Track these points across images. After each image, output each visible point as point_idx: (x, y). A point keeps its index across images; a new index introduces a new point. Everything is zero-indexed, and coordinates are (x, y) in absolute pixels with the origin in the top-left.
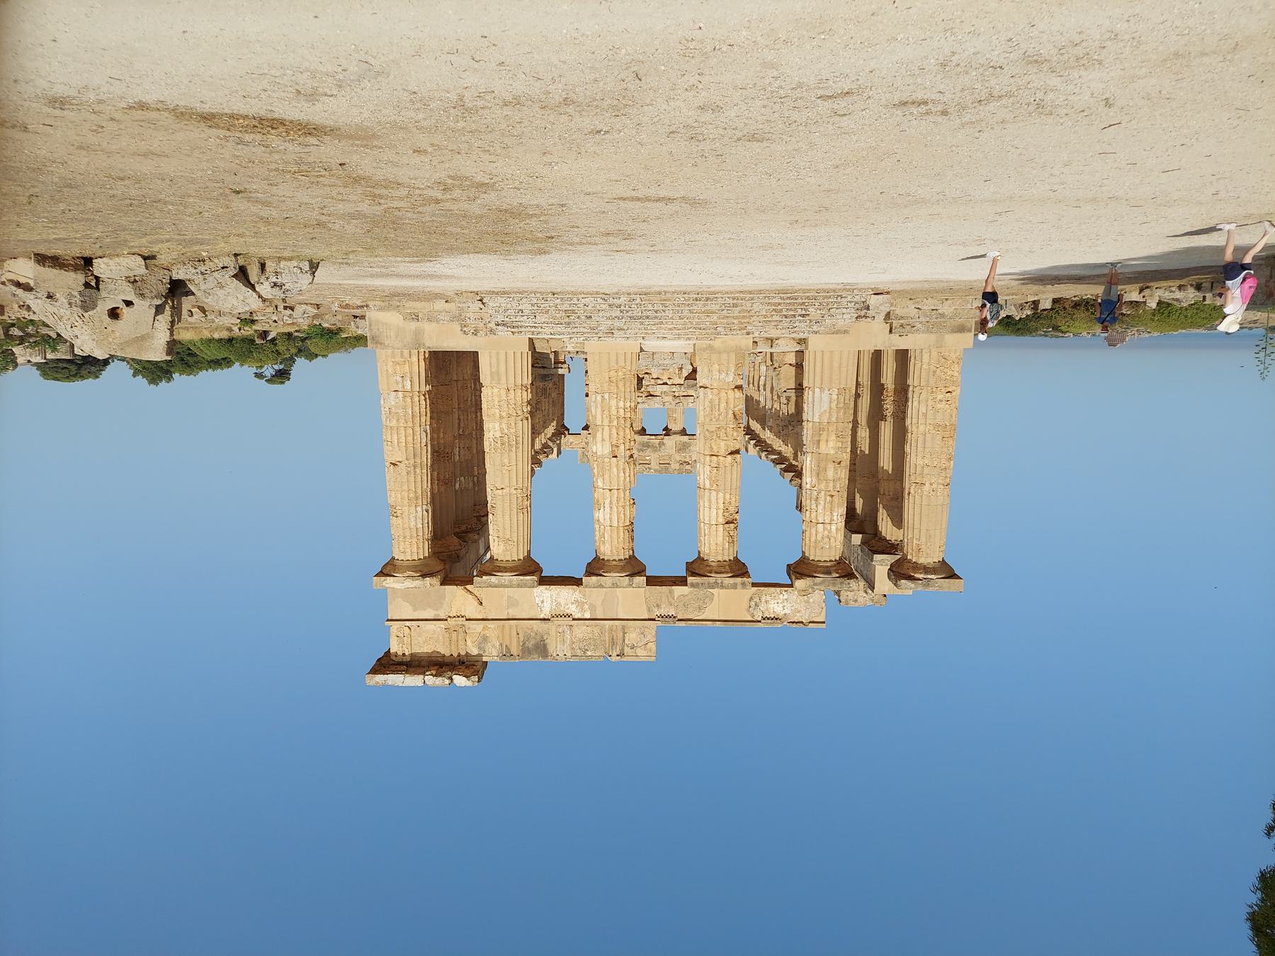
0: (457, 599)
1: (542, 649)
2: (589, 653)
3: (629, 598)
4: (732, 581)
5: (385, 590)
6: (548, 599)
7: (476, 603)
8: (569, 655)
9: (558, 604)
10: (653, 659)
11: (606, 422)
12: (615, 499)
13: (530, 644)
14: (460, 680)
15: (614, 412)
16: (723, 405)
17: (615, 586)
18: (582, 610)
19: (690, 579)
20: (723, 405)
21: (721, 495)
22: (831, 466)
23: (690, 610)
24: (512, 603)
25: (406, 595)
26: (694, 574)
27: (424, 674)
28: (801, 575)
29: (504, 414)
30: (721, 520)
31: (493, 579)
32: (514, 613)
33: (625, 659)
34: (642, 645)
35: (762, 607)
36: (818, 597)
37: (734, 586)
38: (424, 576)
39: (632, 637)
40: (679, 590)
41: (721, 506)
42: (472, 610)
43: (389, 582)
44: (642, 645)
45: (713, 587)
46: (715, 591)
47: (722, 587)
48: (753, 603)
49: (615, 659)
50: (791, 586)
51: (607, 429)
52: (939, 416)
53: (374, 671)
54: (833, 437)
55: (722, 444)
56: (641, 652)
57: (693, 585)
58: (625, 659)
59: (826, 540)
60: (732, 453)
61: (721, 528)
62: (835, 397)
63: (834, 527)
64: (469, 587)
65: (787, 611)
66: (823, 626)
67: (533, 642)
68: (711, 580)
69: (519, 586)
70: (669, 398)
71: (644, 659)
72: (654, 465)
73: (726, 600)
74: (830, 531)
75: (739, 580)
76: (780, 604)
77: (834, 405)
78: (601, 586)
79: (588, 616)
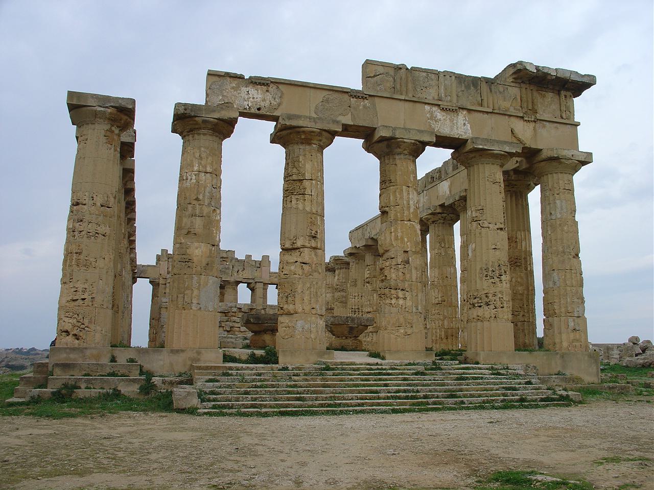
4: (300, 123)
7: (516, 131)
9: (451, 121)
12: (406, 213)
16: (306, 298)
17: (408, 130)
18: (432, 113)
20: (306, 298)
51: (414, 279)
54: (195, 259)
57: (338, 122)
59: (204, 155)
61: (308, 176)
62: (195, 301)
63: (196, 168)
65: (244, 89)
74: (200, 164)
75: (294, 123)
77: (196, 292)
79: (427, 107)
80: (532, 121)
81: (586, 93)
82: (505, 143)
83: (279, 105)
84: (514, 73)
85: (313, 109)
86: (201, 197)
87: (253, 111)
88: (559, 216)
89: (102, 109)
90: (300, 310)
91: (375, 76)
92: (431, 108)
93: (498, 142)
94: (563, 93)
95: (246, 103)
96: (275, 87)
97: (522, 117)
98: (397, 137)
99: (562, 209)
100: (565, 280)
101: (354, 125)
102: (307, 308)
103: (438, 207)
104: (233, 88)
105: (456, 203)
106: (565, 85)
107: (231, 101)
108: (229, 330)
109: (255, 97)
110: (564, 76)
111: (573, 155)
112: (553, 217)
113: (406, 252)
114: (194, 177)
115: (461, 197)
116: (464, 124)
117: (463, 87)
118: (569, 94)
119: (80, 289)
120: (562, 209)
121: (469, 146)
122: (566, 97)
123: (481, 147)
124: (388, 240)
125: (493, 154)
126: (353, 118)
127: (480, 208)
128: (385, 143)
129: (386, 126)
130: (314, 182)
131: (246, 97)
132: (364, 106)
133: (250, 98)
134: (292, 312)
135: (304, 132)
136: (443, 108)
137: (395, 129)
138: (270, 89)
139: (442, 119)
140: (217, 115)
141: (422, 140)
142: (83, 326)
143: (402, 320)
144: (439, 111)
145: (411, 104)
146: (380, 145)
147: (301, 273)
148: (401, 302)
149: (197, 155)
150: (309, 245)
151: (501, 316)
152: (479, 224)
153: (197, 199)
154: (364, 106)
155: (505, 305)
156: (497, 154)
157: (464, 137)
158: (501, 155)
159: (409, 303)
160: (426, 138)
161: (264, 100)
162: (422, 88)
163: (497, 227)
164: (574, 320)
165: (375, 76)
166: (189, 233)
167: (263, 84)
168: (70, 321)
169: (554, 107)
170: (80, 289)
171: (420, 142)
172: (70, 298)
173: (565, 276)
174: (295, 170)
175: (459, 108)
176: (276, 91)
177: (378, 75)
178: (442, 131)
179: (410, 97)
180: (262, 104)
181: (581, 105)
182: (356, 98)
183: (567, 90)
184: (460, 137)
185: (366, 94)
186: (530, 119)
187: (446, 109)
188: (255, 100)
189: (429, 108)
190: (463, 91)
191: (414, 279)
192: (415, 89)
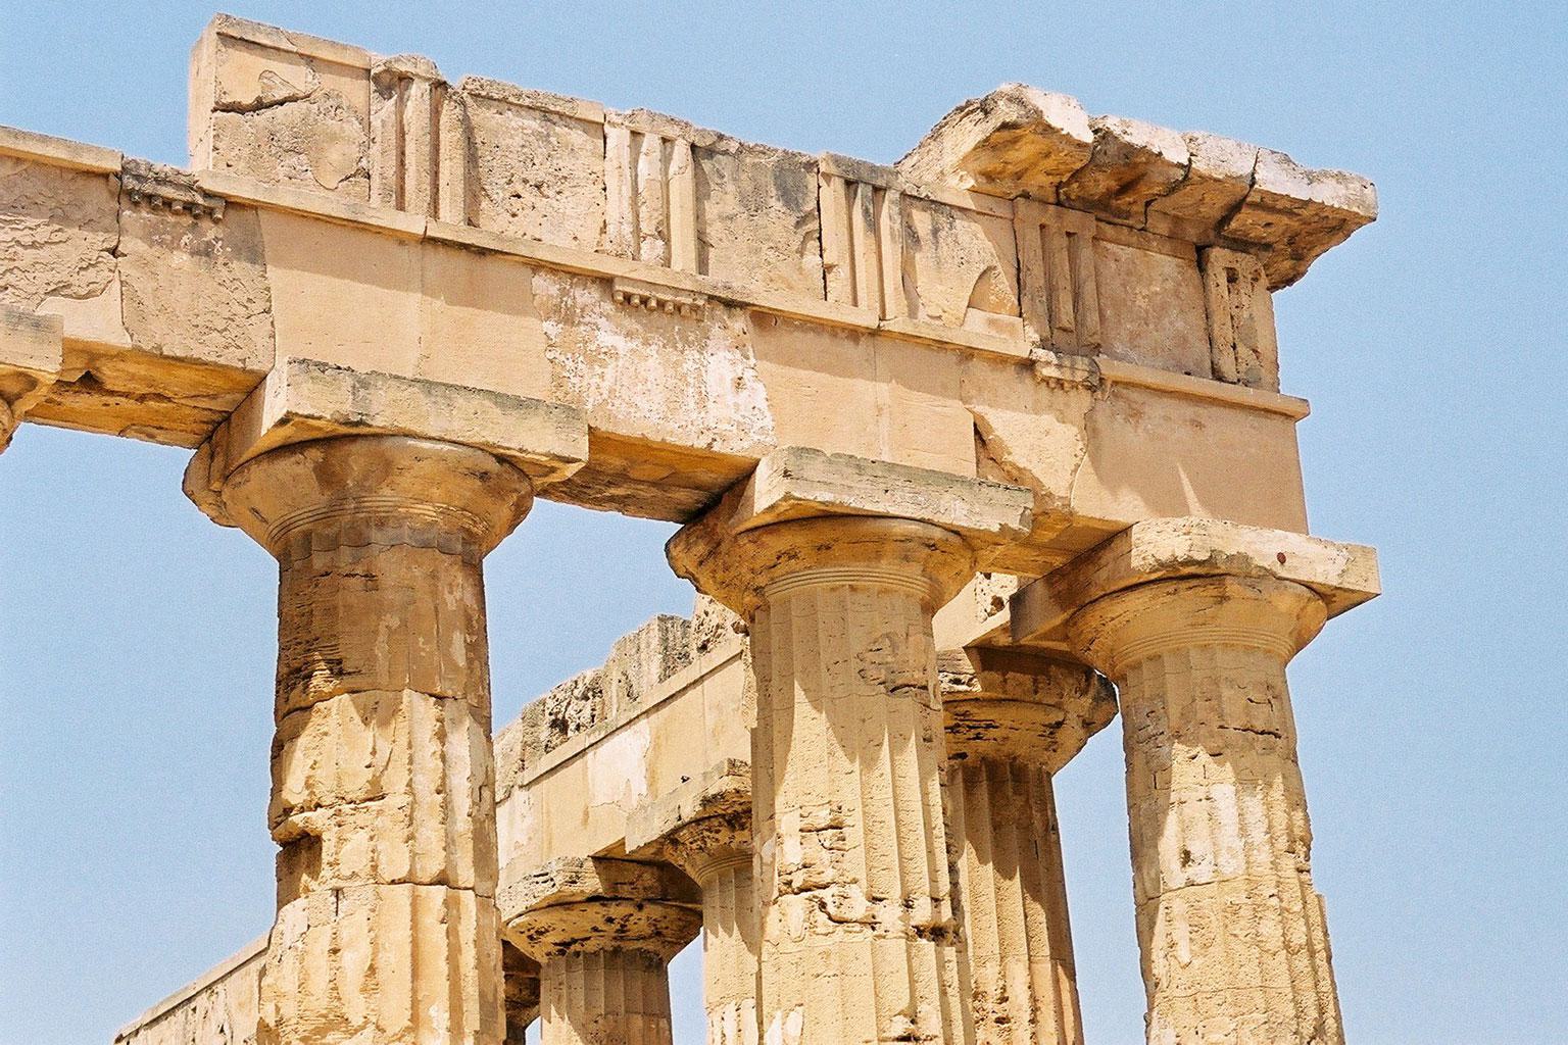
57: (41, 326)
80: (1074, 386)
81: (1325, 266)
82: (951, 480)
84: (986, 144)
91: (259, 106)
92: (564, 292)
94: (1219, 257)
97: (1028, 365)
98: (379, 422)
103: (590, 864)
105: (684, 835)
106: (1225, 220)
111: (1282, 558)
112: (1201, 871)
115: (706, 802)
117: (729, 198)
118: (1245, 263)
121: (765, 493)
122: (1232, 278)
123: (822, 496)
124: (319, 984)
127: (823, 817)
128: (315, 454)
129: (323, 367)
136: (628, 298)
144: (608, 307)
145: (461, 260)
146: (285, 466)
152: (823, 906)
157: (736, 447)
160: (536, 439)
162: (519, 188)
165: (259, 106)
169: (1180, 325)
175: (711, 298)
177: (281, 103)
178: (620, 409)
179: (450, 223)
181: (1307, 323)
182: (155, 209)
183: (1240, 244)
184: (716, 447)
185: (207, 195)
186: (1067, 375)
187: (644, 301)
189: (554, 290)
190: (731, 218)
192: (474, 191)
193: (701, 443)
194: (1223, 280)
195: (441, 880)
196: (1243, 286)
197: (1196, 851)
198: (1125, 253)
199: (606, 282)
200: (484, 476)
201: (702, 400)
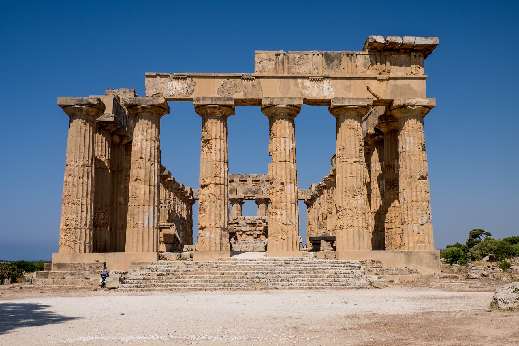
0: (383, 90)
1: (329, 59)
2: (298, 56)
3: (272, 92)
4: (206, 102)
5: (428, 96)
6: (326, 90)
8: (311, 55)
9: (318, 87)
10: (256, 52)
11: (289, 205)
12: (283, 155)
13: (336, 62)
14: (380, 39)
15: (284, 212)
17: (282, 99)
19: (232, 103)
20: (213, 216)
21: (213, 158)
22: (143, 178)
23: (233, 83)
24: (348, 88)
25: (415, 94)
26: (230, 107)
27: (402, 44)
28: (160, 106)
29: (355, 210)
30: (213, 142)
31: (360, 103)
32: (348, 82)
33: (275, 52)
34: (264, 61)
35: (186, 86)
36: (150, 92)
37: (204, 99)
38: (404, 106)
39: (271, 65)
40: (240, 96)
41: (213, 151)
42: (374, 85)
43: (425, 102)
44: (264, 61)
45: (218, 98)
46: (217, 95)
47: (212, 98)
48: (192, 88)
49: (282, 52)
50: (167, 100)
52: (74, 209)
53: (433, 46)
55: (212, 192)
56: (265, 57)
57: (231, 99)
58: (275, 52)
60: (206, 186)
61: (213, 136)
62: (140, 222)
64: (376, 99)
65: (170, 83)
66: (147, 74)
67: (334, 63)
68: (219, 103)
69: (344, 99)
70: (241, 222)
71: (263, 52)
72: (250, 180)
73: (210, 90)
75: (201, 103)
76: (173, 88)
77: (141, 217)
78: (291, 99)
79: (299, 80)
82: (359, 99)
83: (193, 91)
85: (216, 91)
86: (143, 156)
87: (175, 97)
88: (408, 149)
89: (79, 106)
90: (208, 225)
93: (352, 99)
95: (171, 92)
96: (190, 79)
98: (274, 104)
99: (410, 144)
100: (411, 196)
101: (245, 99)
102: (213, 224)
104: (162, 83)
107: (161, 92)
108: (256, 237)
109: (177, 87)
110: (409, 42)
112: (404, 150)
113: (282, 183)
114: (139, 144)
116: (329, 89)
118: (418, 54)
119: (70, 218)
120: (410, 144)
122: (415, 56)
123: (338, 104)
125: (349, 108)
126: (245, 95)
130: (218, 140)
131: (171, 88)
132: (253, 86)
133: (173, 88)
134: (204, 227)
135: (210, 108)
137: (272, 99)
138: (187, 81)
139: (311, 86)
140: (150, 103)
141: (292, 104)
142: (72, 240)
143: (279, 229)
147: (209, 201)
148: (279, 217)
149: (141, 129)
150: (214, 183)
151: (356, 225)
153: (141, 158)
154: (253, 86)
155: (360, 217)
156: (352, 108)
157: (328, 98)
158: (355, 108)
159: (284, 218)
161: (183, 89)
163: (354, 160)
164: (418, 227)
166: (136, 180)
167: (182, 78)
168: (65, 237)
170: (70, 218)
171: (291, 106)
172: (64, 224)
173: (412, 194)
174: (206, 133)
176: (190, 81)
178: (310, 96)
180: (182, 92)
188: (177, 89)
191: (289, 201)
193: (322, 98)
194: (413, 57)
195: (285, 161)
196: (417, 58)
197: (404, 147)
198: (396, 56)
199: (308, 78)
200: (289, 108)
201: (323, 92)
